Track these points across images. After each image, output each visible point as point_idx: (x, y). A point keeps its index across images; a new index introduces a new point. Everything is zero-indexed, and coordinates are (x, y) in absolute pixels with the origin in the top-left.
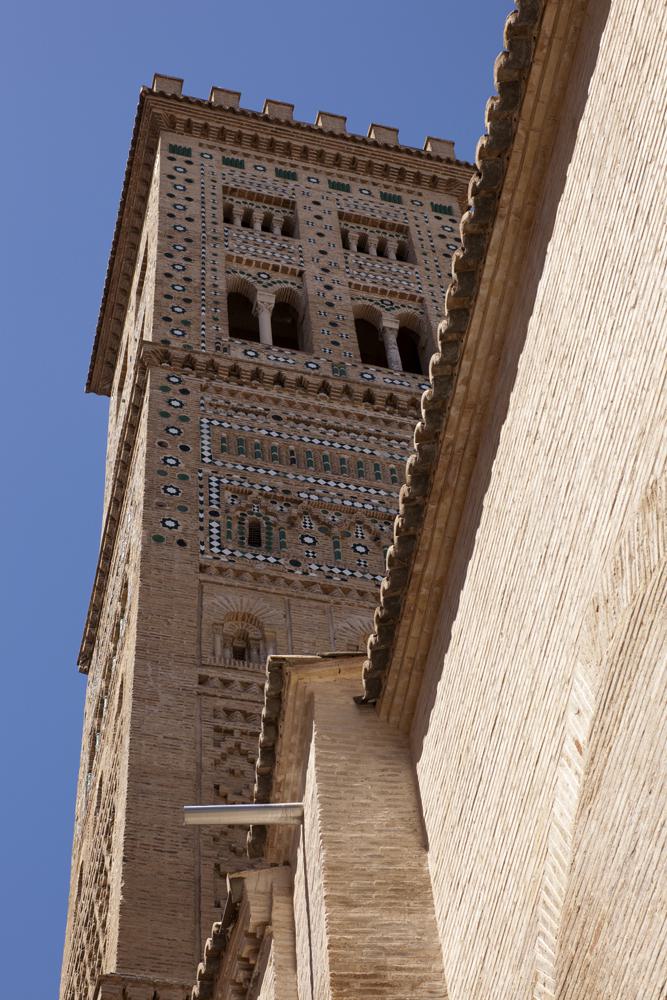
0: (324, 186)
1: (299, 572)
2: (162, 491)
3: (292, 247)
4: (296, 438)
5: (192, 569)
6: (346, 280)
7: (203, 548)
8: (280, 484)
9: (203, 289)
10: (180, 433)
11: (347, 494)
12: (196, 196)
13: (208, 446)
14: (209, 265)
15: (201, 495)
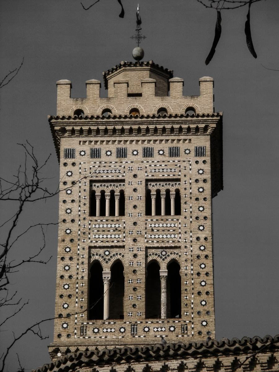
0: (140, 157)
9: (77, 283)
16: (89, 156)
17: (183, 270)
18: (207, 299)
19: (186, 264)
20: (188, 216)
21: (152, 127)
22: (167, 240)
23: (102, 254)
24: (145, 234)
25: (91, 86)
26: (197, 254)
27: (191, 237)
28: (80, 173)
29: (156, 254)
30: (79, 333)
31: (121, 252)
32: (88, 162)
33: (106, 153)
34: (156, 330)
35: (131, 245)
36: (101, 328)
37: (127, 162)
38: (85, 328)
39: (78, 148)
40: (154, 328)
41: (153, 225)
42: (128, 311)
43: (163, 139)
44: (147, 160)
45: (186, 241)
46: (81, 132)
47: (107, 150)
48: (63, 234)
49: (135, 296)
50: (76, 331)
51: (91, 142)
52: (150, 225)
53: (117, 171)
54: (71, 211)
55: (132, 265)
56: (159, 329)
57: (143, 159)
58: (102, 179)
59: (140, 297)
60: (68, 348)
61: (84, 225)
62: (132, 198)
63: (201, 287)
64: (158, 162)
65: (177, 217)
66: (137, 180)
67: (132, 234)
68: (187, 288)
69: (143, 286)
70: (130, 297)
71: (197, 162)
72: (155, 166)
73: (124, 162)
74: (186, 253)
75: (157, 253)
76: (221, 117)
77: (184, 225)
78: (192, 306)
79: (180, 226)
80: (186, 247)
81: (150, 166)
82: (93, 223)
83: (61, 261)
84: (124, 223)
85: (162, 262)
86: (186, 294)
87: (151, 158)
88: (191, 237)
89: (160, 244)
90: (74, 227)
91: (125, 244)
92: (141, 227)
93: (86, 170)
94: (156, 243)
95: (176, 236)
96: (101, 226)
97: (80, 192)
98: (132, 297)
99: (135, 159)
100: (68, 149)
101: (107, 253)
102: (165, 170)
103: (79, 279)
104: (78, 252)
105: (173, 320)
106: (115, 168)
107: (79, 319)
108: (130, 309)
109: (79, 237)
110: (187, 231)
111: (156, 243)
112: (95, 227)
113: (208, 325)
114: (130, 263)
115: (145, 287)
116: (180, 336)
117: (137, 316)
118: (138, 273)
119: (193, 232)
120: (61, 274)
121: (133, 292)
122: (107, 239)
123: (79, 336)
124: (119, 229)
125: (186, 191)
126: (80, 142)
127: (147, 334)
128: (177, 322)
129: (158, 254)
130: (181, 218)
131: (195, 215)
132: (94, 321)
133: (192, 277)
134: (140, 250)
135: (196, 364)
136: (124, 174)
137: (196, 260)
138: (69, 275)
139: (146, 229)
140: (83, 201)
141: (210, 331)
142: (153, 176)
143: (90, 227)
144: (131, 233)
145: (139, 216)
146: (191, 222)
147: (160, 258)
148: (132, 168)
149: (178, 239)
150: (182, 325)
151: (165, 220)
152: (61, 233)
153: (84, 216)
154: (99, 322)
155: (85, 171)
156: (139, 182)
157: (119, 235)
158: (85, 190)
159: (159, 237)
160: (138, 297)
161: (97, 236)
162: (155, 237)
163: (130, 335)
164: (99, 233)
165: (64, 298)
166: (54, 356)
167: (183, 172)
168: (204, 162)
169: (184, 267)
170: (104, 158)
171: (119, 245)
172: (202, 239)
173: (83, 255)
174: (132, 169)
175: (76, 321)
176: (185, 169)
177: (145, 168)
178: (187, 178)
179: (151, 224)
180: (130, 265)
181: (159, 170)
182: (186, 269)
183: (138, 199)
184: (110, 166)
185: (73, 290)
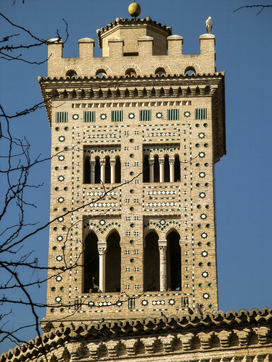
0: (137, 121)
17: (182, 241)
18: (209, 270)
19: (186, 234)
20: (188, 183)
21: (149, 88)
22: (166, 208)
23: (98, 224)
25: (84, 45)
26: (198, 223)
27: (192, 205)
28: (73, 138)
29: (154, 224)
31: (117, 222)
32: (81, 126)
33: (101, 117)
34: (154, 303)
35: (127, 214)
36: (96, 302)
37: (123, 126)
39: (71, 111)
40: (153, 302)
41: (151, 193)
42: (125, 283)
43: (161, 101)
44: (145, 124)
45: (186, 210)
46: (74, 94)
47: (102, 113)
48: (55, 203)
49: (133, 268)
51: (84, 105)
52: (148, 193)
53: (113, 136)
54: (64, 178)
55: (129, 235)
56: (158, 303)
57: (140, 123)
58: (96, 144)
59: (138, 268)
60: (62, 323)
61: (78, 193)
62: (129, 164)
63: (202, 258)
64: (156, 125)
65: (177, 184)
66: (134, 145)
67: (129, 202)
68: (187, 259)
69: (141, 257)
70: (127, 269)
71: (197, 125)
72: (153, 129)
73: (120, 126)
74: (186, 221)
75: (156, 222)
76: (223, 77)
77: (184, 193)
78: (193, 278)
79: (179, 193)
80: (186, 215)
81: (148, 130)
82: (87, 190)
83: (54, 231)
84: (121, 190)
85: (161, 231)
86: (186, 266)
87: (148, 122)
88: (192, 205)
89: (159, 213)
90: (68, 196)
91: (121, 212)
92: (138, 195)
93: (79, 135)
94: (154, 212)
95: (176, 204)
96: (96, 194)
97: (73, 158)
98: (129, 269)
99: (132, 123)
101: (102, 222)
102: (163, 135)
103: (72, 250)
105: (173, 292)
106: (110, 132)
107: (73, 293)
108: (127, 281)
110: (187, 199)
111: (154, 212)
112: (90, 195)
113: (211, 297)
114: (127, 233)
116: (180, 309)
118: (136, 243)
119: (193, 199)
120: (54, 245)
121: (130, 263)
122: (102, 208)
124: (115, 197)
125: (186, 156)
126: (73, 105)
127: (146, 308)
128: (177, 294)
129: (157, 224)
130: (181, 185)
131: (196, 182)
133: (193, 247)
134: (138, 219)
135: (191, 338)
136: (120, 139)
137: (197, 229)
139: (144, 196)
140: (76, 168)
141: (212, 304)
142: (150, 140)
143: (84, 195)
144: (127, 201)
145: (136, 183)
146: (191, 189)
147: (158, 228)
148: (128, 132)
150: (182, 298)
152: (53, 203)
153: (78, 184)
154: (95, 295)
155: (79, 136)
156: (136, 147)
157: (115, 204)
158: (78, 156)
159: (157, 206)
160: (136, 268)
162: (153, 206)
167: (183, 136)
168: (205, 125)
169: (184, 236)
170: (98, 122)
171: (115, 214)
172: (203, 207)
174: (128, 133)
175: (70, 294)
176: (185, 133)
177: (142, 132)
178: (187, 143)
179: (149, 192)
180: (127, 235)
181: (157, 134)
182: (187, 239)
183: (135, 165)
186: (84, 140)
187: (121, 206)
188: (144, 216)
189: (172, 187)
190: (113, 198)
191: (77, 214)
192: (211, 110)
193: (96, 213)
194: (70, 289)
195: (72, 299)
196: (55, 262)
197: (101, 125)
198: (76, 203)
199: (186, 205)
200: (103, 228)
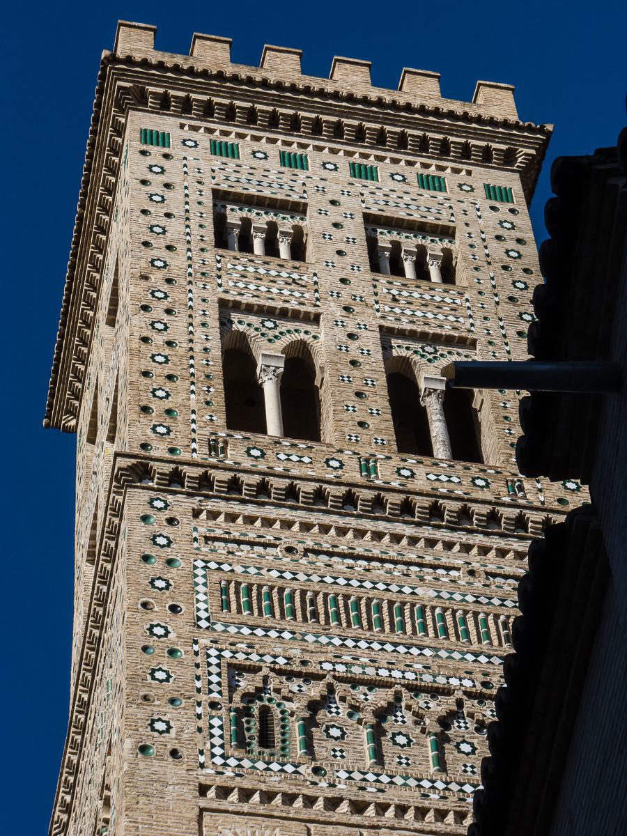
0: (344, 174)
1: (324, 784)
2: (149, 677)
3: (305, 278)
4: (315, 578)
5: (190, 792)
6: (375, 323)
7: (202, 759)
8: (296, 652)
9: (192, 357)
10: (168, 585)
11: (383, 660)
12: (178, 210)
13: (205, 602)
14: (198, 320)
15: (198, 678)
16: (209, 151)
24: (374, 303)
27: (502, 328)
30: (206, 451)
38: (221, 445)
40: (427, 474)
41: (394, 292)
50: (194, 445)
52: (386, 291)
53: (286, 187)
55: (347, 351)
57: (352, 180)
58: (245, 192)
62: (332, 237)
67: (338, 297)
69: (385, 392)
74: (494, 352)
77: (481, 306)
79: (468, 304)
80: (490, 343)
82: (226, 260)
83: (142, 312)
88: (502, 328)
91: (320, 310)
100: (152, 131)
101: (269, 324)
104: (190, 303)
106: (279, 180)
109: (189, 279)
115: (390, 395)
117: (373, 444)
120: (145, 334)
123: (205, 456)
124: (303, 283)
132: (248, 435)
134: (366, 329)
136: (305, 195)
138: (166, 339)
149: (468, 326)
151: (427, 288)
153: (203, 245)
155: (199, 172)
157: (303, 294)
161: (241, 285)
163: (359, 476)
164: (247, 279)
165: (154, 378)
166: (132, 481)
168: (512, 211)
173: (204, 311)
175: (193, 426)
184: (267, 176)
185: (179, 368)
186: (214, 181)
187: (318, 299)
188: (381, 327)
189: (448, 292)
190: (297, 284)
191: (203, 294)
192: (521, 193)
193: (254, 301)
194: (193, 416)
195: (198, 434)
196: (148, 363)
197: (254, 166)
198: (199, 275)
199: (489, 325)
200: (271, 334)
